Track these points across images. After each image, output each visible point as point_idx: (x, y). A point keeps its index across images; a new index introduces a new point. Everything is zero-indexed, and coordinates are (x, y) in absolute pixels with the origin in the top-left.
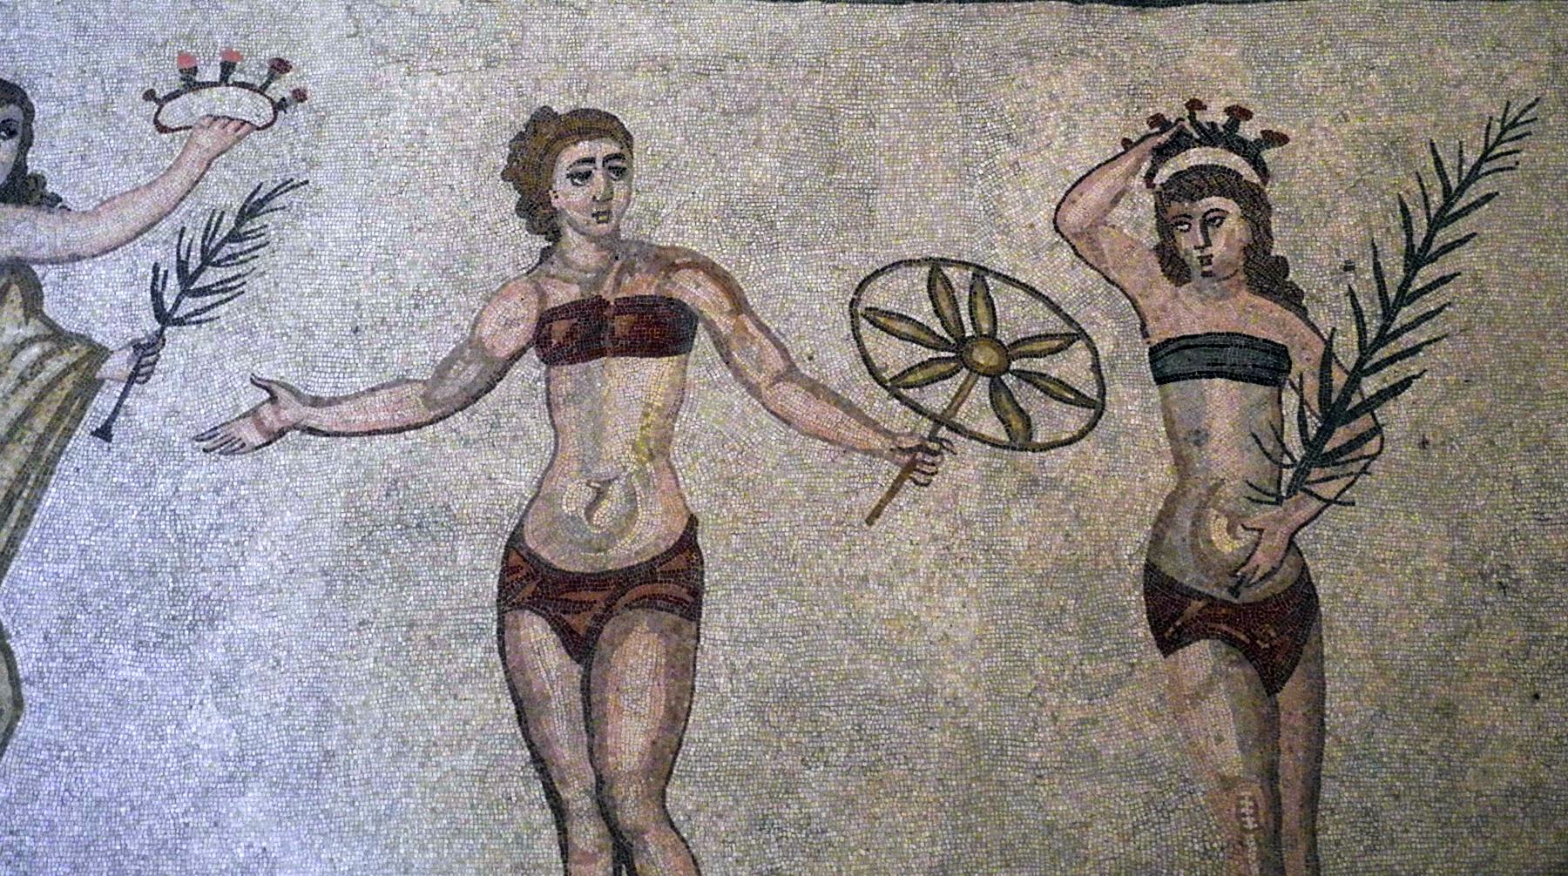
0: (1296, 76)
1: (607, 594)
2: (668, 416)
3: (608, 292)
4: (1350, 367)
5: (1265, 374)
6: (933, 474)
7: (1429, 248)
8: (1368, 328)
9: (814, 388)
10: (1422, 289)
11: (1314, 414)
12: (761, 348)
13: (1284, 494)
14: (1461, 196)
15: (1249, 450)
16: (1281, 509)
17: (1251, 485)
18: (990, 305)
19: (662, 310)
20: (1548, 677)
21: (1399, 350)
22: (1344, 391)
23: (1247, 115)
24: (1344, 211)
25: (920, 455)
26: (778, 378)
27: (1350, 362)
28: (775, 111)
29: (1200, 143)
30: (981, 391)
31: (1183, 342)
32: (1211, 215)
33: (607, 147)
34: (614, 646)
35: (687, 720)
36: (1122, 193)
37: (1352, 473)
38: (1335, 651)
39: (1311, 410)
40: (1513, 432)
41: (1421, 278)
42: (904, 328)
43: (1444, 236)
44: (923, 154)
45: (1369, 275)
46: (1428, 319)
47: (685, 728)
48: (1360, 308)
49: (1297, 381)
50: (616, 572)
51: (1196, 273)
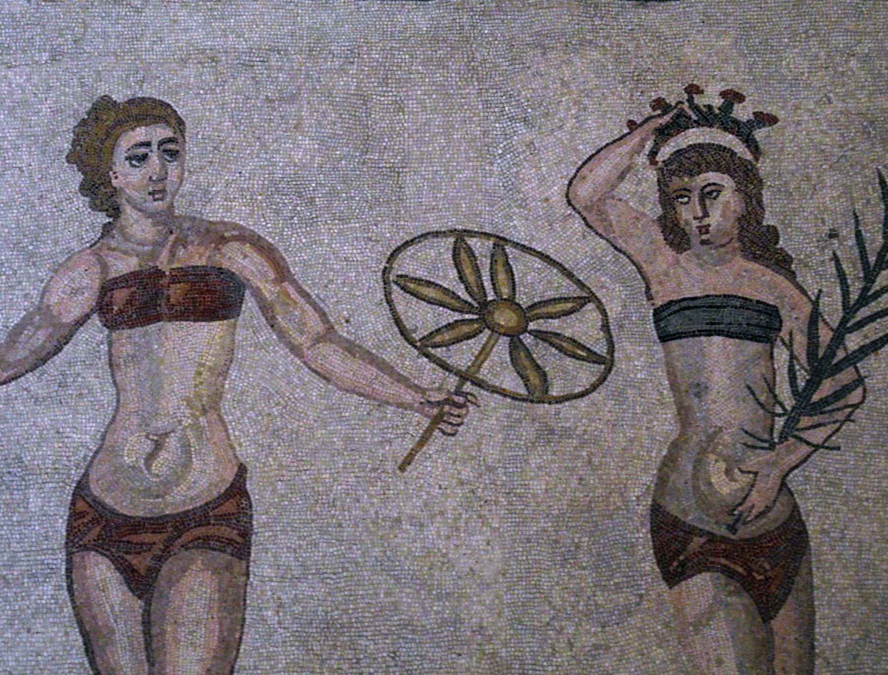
0: (784, 63)
1: (164, 536)
2: (219, 374)
3: (163, 263)
4: (835, 325)
5: (757, 332)
6: (459, 425)
9: (351, 348)
11: (803, 368)
12: (303, 311)
13: (776, 440)
15: (744, 400)
16: (773, 454)
17: (746, 432)
18: (510, 271)
19: (213, 278)
21: (879, 309)
22: (829, 347)
23: (740, 98)
24: (828, 184)
25: (447, 408)
26: (319, 339)
27: (835, 320)
28: (314, 98)
29: (698, 124)
30: (502, 347)
31: (684, 304)
32: (708, 189)
33: (161, 132)
34: (171, 583)
35: (238, 650)
36: (629, 169)
37: (837, 421)
38: (824, 582)
39: (800, 364)
42: (430, 292)
44: (447, 135)
45: (852, 242)
47: (237, 657)
48: (843, 272)
49: (787, 338)
50: (172, 516)
51: (695, 241)
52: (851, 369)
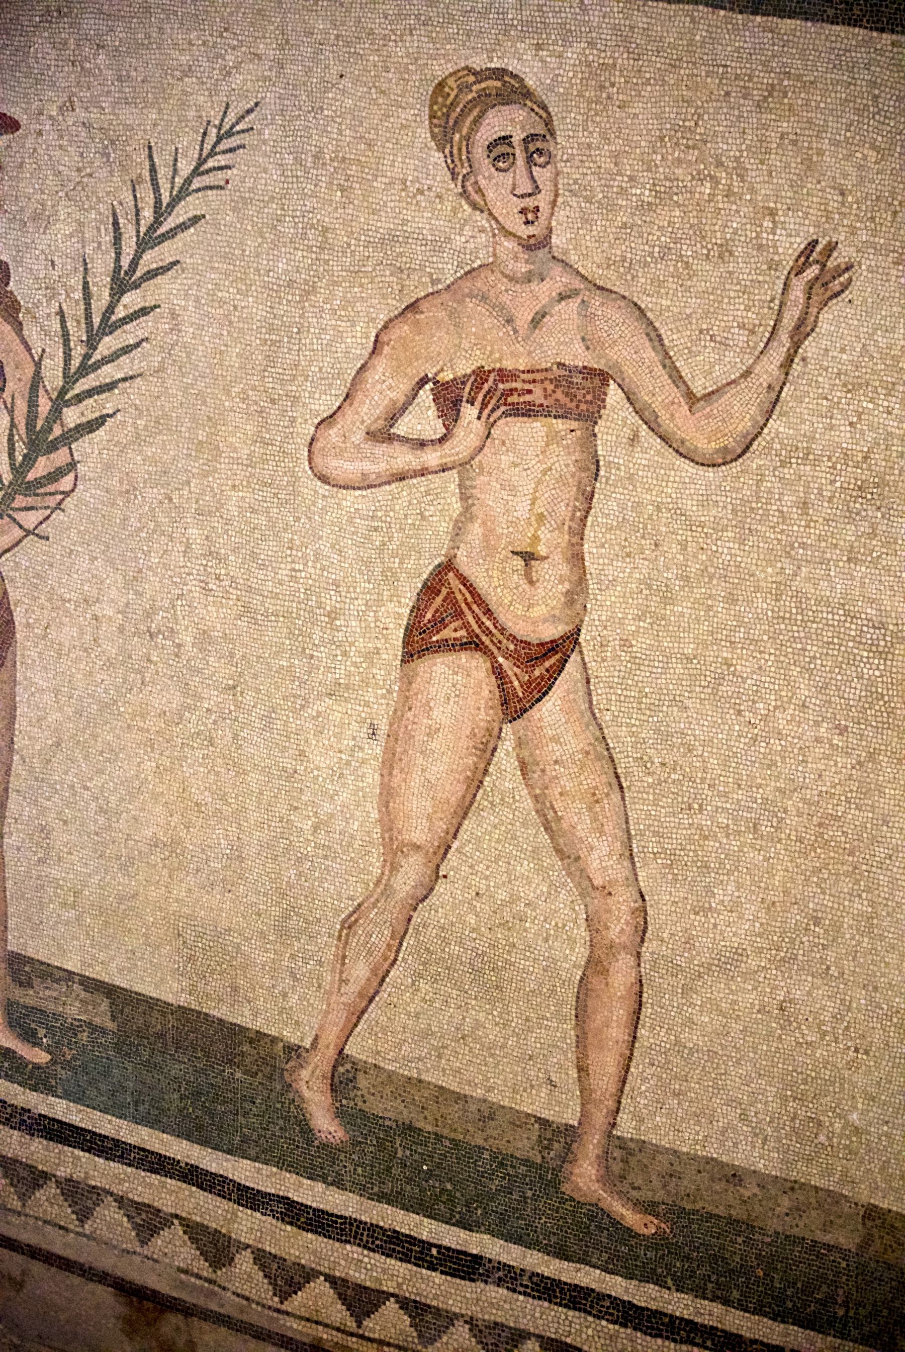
7: (134, 272)
8: (73, 353)
10: (124, 318)
11: (21, 439)
14: (170, 214)
20: (195, 745)
21: (98, 384)
38: (25, 679)
40: (190, 492)
41: (125, 306)
43: (150, 259)
45: (78, 295)
46: (126, 353)
52: (66, 450)
